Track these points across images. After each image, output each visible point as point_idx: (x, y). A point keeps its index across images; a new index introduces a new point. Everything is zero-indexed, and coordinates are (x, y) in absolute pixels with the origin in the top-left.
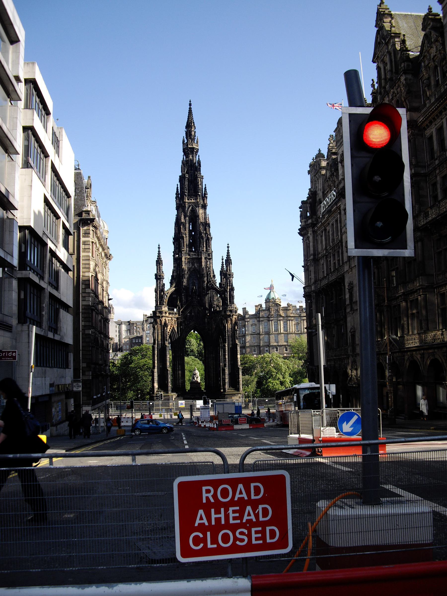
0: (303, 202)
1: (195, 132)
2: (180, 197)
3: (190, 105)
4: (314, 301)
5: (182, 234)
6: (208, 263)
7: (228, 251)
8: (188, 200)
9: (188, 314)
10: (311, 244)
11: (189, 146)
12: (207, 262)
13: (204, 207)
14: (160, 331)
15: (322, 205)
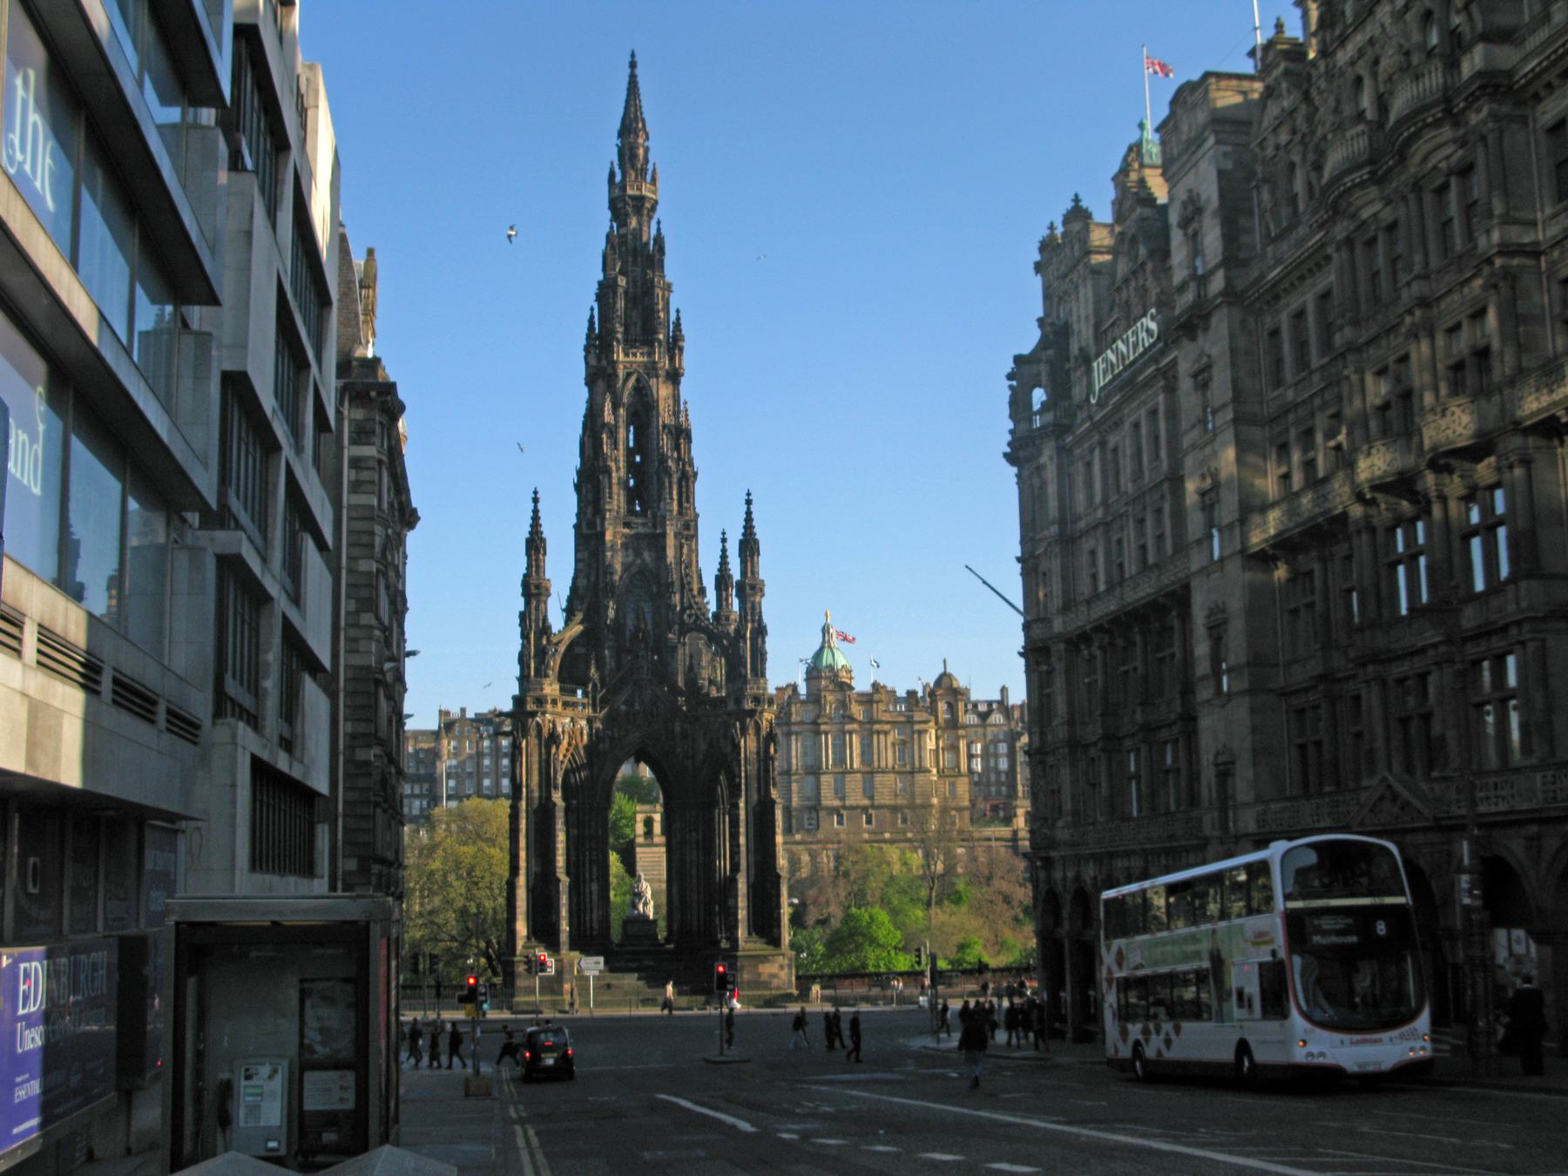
0: (1018, 360)
1: (647, 150)
2: (599, 345)
3: (633, 65)
4: (1059, 666)
5: (605, 460)
6: (685, 550)
7: (749, 513)
8: (627, 355)
9: (623, 708)
10: (1052, 489)
11: (630, 192)
12: (681, 547)
13: (674, 377)
14: (535, 758)
15: (1098, 365)
